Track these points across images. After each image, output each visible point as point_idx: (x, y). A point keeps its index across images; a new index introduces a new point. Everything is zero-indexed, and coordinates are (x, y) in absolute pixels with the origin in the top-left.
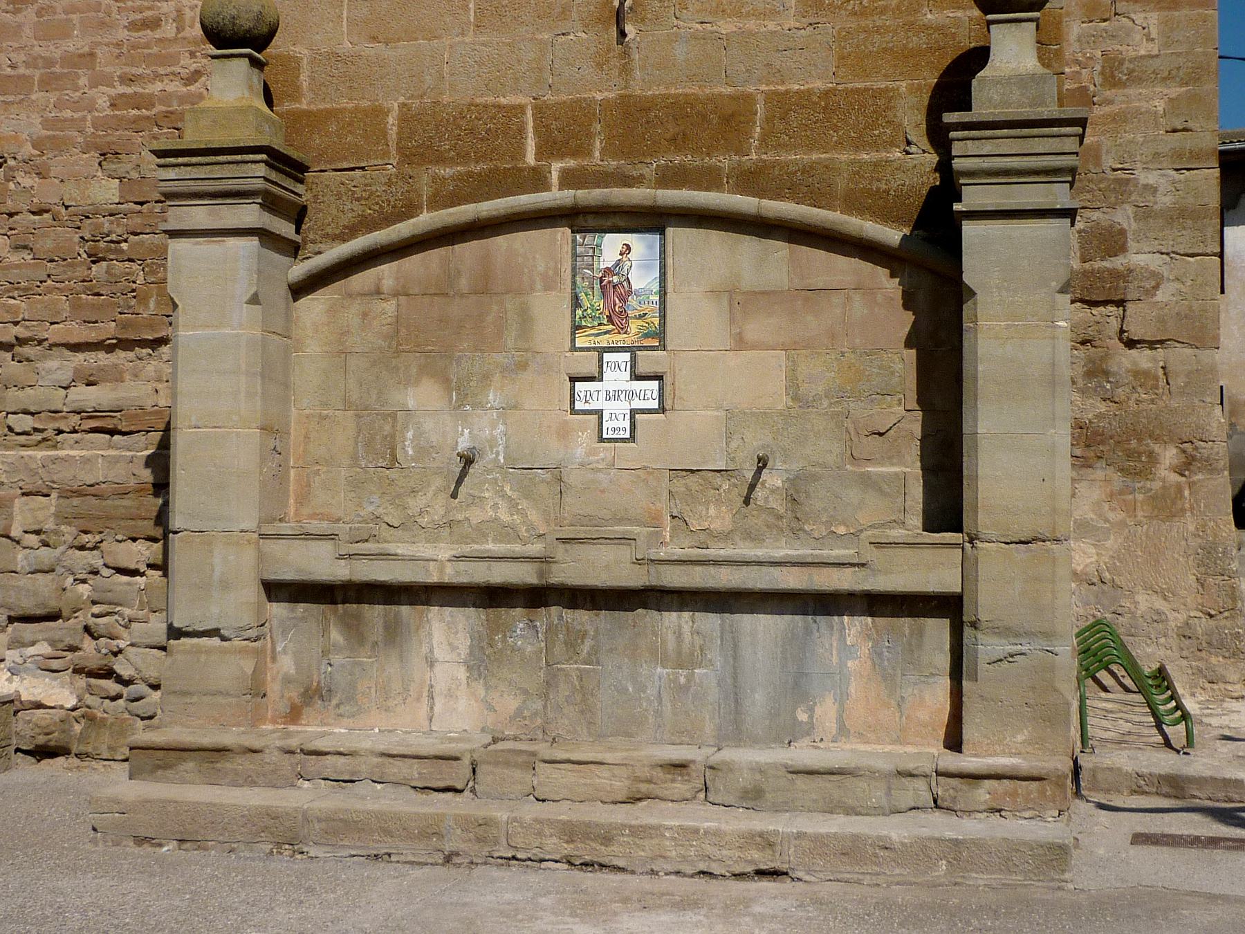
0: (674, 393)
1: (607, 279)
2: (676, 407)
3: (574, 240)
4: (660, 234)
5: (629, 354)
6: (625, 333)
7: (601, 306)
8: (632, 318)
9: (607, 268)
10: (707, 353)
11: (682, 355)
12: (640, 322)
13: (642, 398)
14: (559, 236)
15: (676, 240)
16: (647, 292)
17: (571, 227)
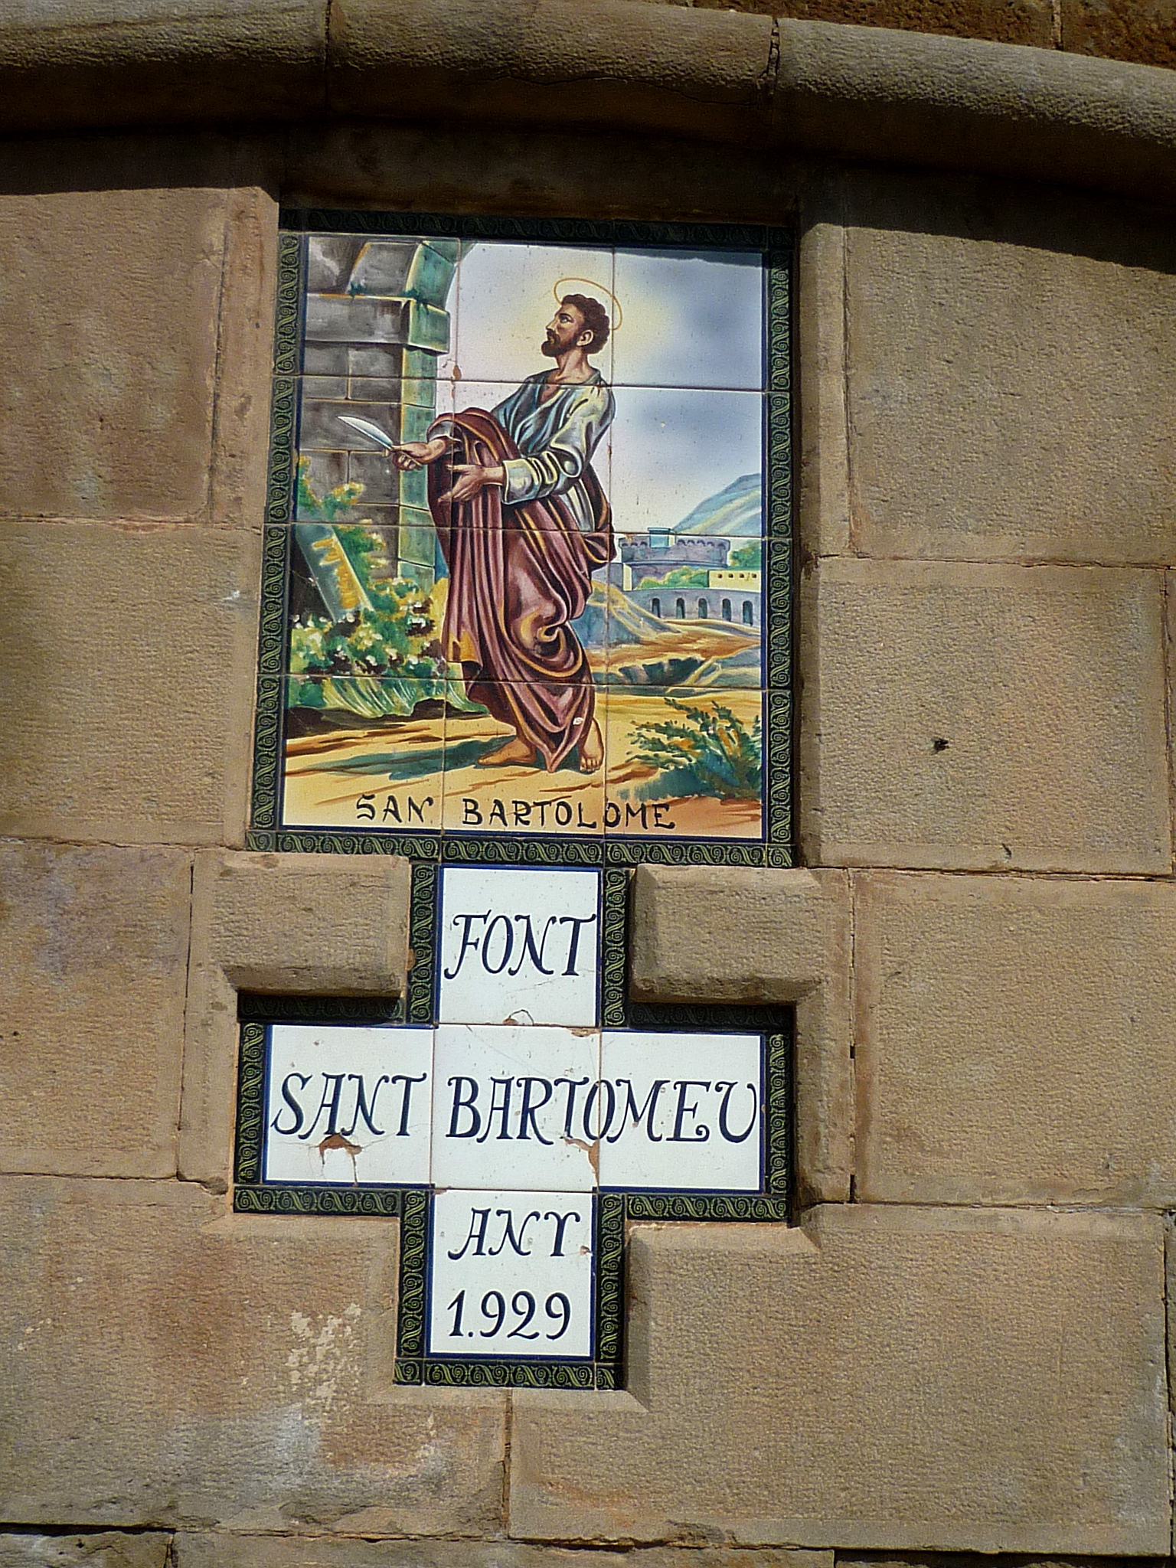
0: (863, 1103)
1: (469, 472)
2: (875, 1185)
3: (294, 265)
4: (767, 263)
5: (591, 879)
6: (571, 762)
7: (438, 612)
8: (611, 681)
9: (473, 414)
10: (1047, 886)
11: (905, 889)
12: (655, 709)
13: (664, 1124)
14: (215, 230)
15: (866, 289)
16: (699, 552)
17: (281, 190)
